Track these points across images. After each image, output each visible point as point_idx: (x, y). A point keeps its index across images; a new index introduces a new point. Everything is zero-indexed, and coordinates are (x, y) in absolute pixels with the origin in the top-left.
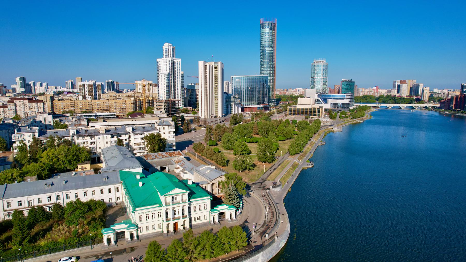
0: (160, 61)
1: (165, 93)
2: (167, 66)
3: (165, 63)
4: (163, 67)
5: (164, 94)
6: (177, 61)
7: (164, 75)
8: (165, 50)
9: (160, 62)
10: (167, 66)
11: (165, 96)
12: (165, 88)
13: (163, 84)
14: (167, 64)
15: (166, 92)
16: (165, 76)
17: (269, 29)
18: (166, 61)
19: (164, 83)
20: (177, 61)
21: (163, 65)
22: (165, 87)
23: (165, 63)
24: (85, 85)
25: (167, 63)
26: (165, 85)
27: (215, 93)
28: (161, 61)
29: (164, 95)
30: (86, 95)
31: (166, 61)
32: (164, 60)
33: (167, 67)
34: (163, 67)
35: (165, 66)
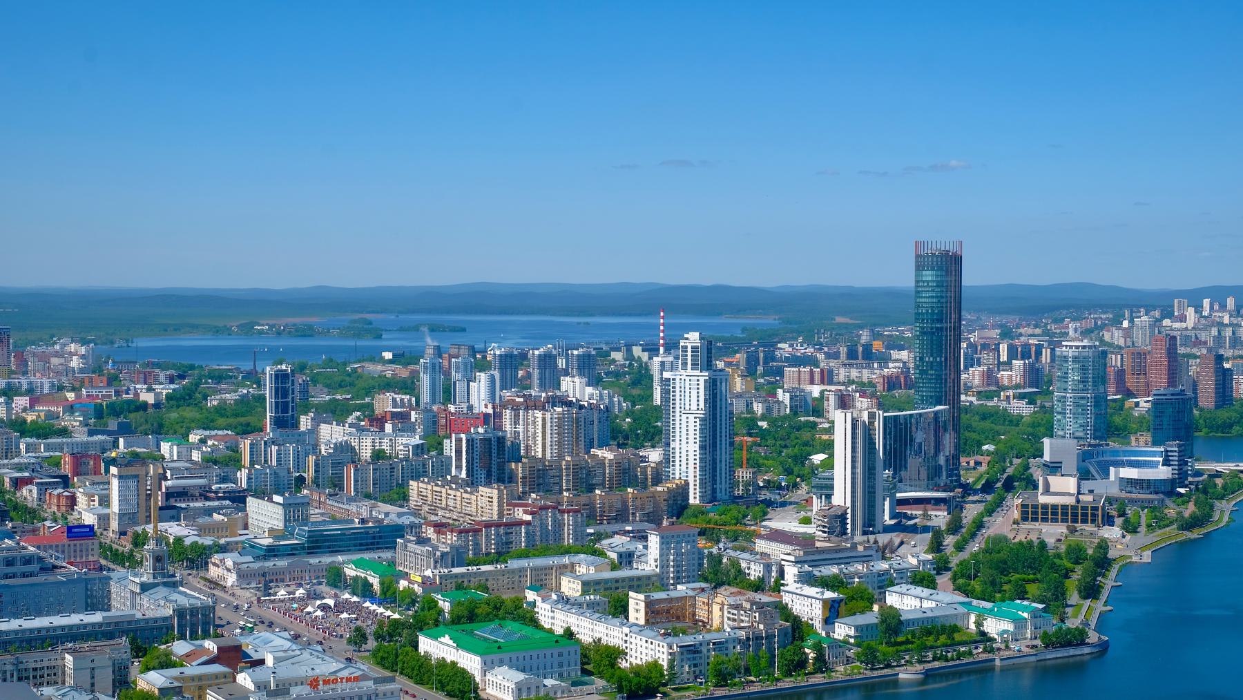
0: (674, 377)
1: (695, 464)
2: (698, 393)
5: (693, 466)
6: (721, 380)
7: (695, 418)
9: (674, 379)
10: (698, 393)
11: (695, 472)
12: (695, 451)
13: (691, 440)
14: (698, 389)
15: (698, 462)
16: (698, 420)
18: (698, 380)
19: (695, 438)
21: (687, 390)
22: (697, 449)
24: (475, 442)
25: (698, 384)
26: (695, 443)
27: (869, 478)
28: (678, 378)
29: (693, 470)
30: (475, 468)
31: (698, 380)
33: (698, 397)
34: (687, 394)
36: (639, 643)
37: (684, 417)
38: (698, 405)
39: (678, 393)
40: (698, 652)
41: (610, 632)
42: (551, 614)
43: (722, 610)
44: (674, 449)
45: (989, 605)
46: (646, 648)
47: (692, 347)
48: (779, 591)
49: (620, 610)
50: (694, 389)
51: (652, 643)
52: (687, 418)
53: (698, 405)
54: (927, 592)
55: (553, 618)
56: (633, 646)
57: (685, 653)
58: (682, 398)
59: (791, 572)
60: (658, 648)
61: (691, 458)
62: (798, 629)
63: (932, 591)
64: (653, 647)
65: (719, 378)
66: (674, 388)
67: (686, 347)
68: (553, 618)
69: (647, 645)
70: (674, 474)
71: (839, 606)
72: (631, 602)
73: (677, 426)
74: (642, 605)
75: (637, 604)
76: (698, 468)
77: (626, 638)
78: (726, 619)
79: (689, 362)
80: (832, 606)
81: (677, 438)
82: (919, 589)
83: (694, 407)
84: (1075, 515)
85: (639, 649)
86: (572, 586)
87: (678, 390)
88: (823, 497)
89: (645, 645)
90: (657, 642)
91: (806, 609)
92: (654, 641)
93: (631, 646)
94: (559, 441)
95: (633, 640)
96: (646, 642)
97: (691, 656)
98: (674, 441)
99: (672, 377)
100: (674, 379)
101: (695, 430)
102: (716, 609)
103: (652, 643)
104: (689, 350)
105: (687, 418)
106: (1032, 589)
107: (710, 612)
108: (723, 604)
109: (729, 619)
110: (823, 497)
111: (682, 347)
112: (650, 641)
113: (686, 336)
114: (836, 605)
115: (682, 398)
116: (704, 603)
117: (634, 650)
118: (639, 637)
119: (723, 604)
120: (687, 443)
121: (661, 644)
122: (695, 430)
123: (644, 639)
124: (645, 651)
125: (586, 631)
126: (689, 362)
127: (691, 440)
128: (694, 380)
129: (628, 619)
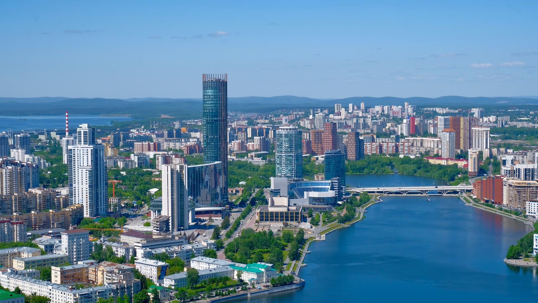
0: (74, 148)
1: (87, 195)
2: (87, 157)
3: (85, 152)
4: (82, 158)
5: (86, 197)
6: (100, 149)
7: (86, 170)
8: (84, 134)
9: (74, 150)
10: (87, 157)
11: (87, 200)
12: (87, 188)
13: (84, 183)
14: (87, 154)
15: (88, 194)
16: (88, 171)
17: (218, 91)
18: (87, 150)
20: (100, 148)
21: (82, 156)
22: (88, 187)
23: (85, 152)
25: (87, 152)
26: (87, 184)
27: (180, 201)
28: (76, 149)
29: (86, 199)
31: (87, 150)
32: (84, 149)
33: (88, 159)
34: (82, 158)
35: (85, 157)
36: (58, 294)
37: (80, 170)
38: (88, 163)
39: (76, 157)
40: (90, 297)
41: (42, 290)
42: (7, 281)
43: (103, 274)
44: (75, 187)
45: (244, 266)
46: (62, 297)
47: (84, 132)
48: (134, 263)
49: (47, 277)
50: (85, 155)
51: (64, 294)
52: (82, 170)
53: (88, 163)
54: (212, 260)
55: (9, 282)
56: (54, 296)
57: (83, 298)
58: (79, 160)
59: (140, 252)
60: (68, 296)
61: (84, 192)
62: (144, 282)
63: (214, 259)
64: (65, 296)
65: (99, 148)
66: (74, 154)
67: (81, 132)
68: (9, 282)
69: (62, 295)
70: (75, 201)
71: (166, 269)
72: (53, 272)
73: (77, 175)
74: (59, 273)
75: (56, 273)
76: (88, 198)
77: (50, 292)
78: (105, 279)
79: (82, 140)
80: (162, 270)
81: (77, 182)
82: (208, 259)
83: (85, 164)
84: (287, 217)
85: (58, 297)
86: (19, 264)
87: (76, 155)
88: (157, 211)
89: (60, 295)
90: (67, 293)
91: (148, 272)
92: (66, 293)
93: (53, 296)
94: (10, 185)
95: (54, 293)
96: (62, 293)
97: (86, 300)
98: (75, 183)
99: (73, 149)
100: (74, 150)
101: (86, 177)
102: (99, 274)
103: (64, 294)
104: (82, 133)
105: (82, 170)
106: (266, 256)
107: (96, 275)
108: (103, 271)
109: (107, 279)
110: (157, 211)
111: (78, 132)
112: (63, 293)
113: (80, 126)
114: (164, 269)
115: (79, 160)
116: (93, 271)
117: (55, 298)
118: (57, 291)
119: (103, 271)
120: (82, 184)
121: (70, 294)
122: (86, 177)
123: (60, 292)
124: (60, 298)
125: (28, 289)
126: (82, 140)
127: (84, 183)
128: (85, 150)
129: (50, 280)
